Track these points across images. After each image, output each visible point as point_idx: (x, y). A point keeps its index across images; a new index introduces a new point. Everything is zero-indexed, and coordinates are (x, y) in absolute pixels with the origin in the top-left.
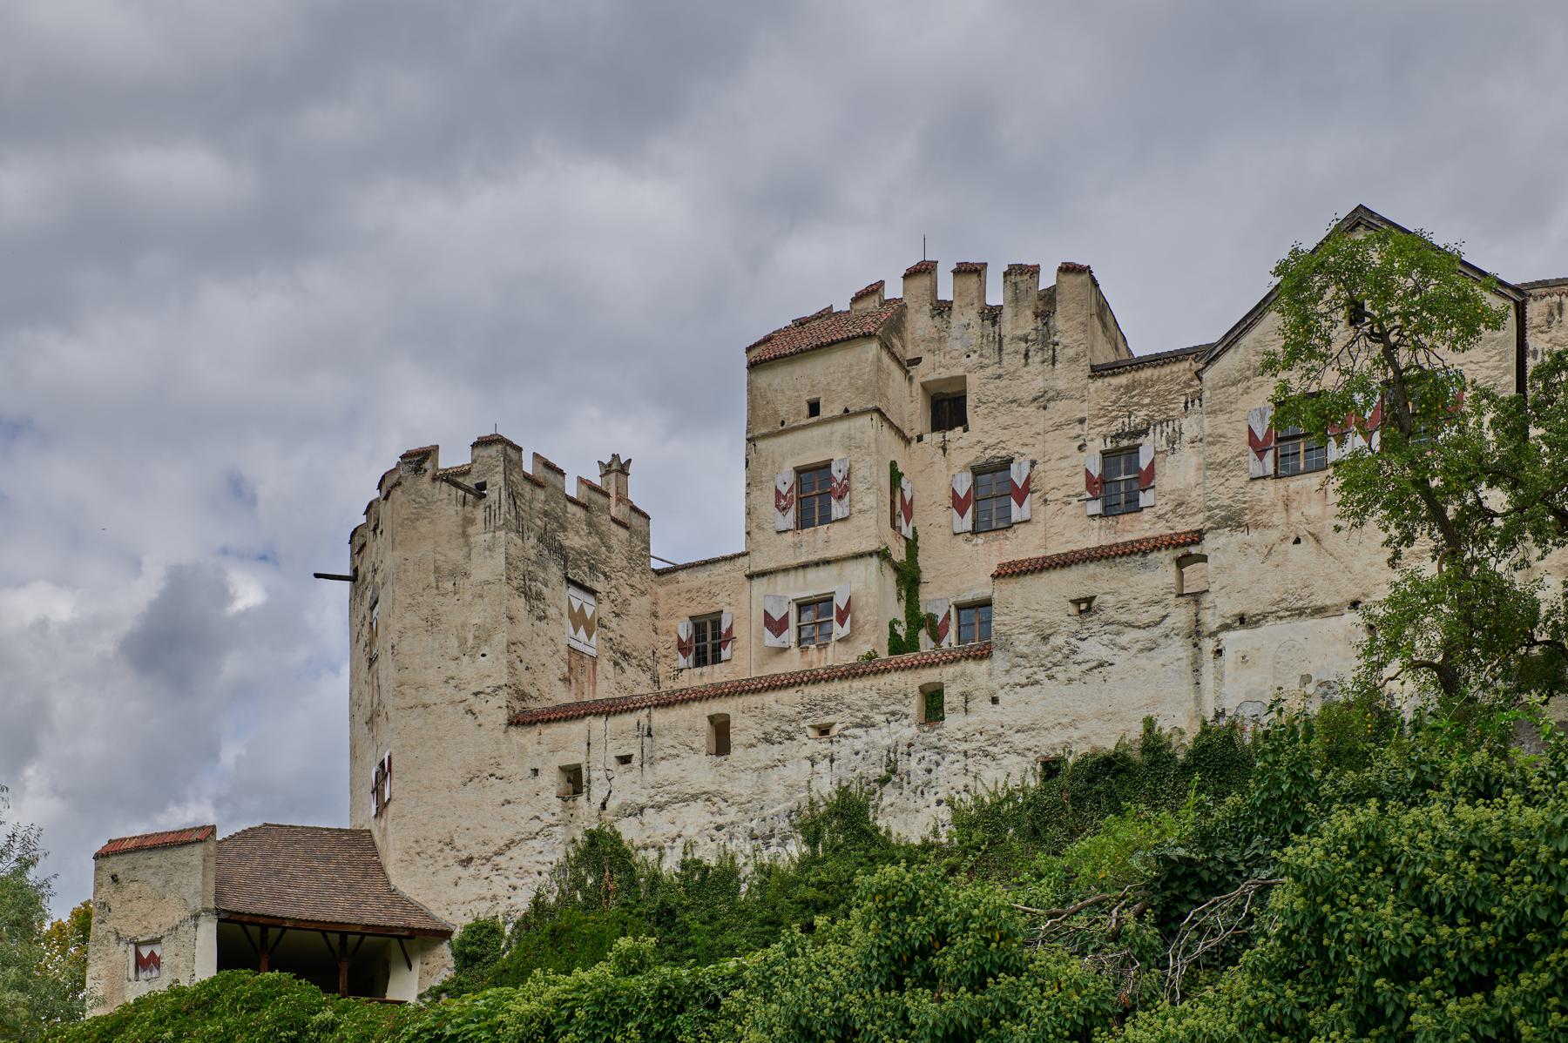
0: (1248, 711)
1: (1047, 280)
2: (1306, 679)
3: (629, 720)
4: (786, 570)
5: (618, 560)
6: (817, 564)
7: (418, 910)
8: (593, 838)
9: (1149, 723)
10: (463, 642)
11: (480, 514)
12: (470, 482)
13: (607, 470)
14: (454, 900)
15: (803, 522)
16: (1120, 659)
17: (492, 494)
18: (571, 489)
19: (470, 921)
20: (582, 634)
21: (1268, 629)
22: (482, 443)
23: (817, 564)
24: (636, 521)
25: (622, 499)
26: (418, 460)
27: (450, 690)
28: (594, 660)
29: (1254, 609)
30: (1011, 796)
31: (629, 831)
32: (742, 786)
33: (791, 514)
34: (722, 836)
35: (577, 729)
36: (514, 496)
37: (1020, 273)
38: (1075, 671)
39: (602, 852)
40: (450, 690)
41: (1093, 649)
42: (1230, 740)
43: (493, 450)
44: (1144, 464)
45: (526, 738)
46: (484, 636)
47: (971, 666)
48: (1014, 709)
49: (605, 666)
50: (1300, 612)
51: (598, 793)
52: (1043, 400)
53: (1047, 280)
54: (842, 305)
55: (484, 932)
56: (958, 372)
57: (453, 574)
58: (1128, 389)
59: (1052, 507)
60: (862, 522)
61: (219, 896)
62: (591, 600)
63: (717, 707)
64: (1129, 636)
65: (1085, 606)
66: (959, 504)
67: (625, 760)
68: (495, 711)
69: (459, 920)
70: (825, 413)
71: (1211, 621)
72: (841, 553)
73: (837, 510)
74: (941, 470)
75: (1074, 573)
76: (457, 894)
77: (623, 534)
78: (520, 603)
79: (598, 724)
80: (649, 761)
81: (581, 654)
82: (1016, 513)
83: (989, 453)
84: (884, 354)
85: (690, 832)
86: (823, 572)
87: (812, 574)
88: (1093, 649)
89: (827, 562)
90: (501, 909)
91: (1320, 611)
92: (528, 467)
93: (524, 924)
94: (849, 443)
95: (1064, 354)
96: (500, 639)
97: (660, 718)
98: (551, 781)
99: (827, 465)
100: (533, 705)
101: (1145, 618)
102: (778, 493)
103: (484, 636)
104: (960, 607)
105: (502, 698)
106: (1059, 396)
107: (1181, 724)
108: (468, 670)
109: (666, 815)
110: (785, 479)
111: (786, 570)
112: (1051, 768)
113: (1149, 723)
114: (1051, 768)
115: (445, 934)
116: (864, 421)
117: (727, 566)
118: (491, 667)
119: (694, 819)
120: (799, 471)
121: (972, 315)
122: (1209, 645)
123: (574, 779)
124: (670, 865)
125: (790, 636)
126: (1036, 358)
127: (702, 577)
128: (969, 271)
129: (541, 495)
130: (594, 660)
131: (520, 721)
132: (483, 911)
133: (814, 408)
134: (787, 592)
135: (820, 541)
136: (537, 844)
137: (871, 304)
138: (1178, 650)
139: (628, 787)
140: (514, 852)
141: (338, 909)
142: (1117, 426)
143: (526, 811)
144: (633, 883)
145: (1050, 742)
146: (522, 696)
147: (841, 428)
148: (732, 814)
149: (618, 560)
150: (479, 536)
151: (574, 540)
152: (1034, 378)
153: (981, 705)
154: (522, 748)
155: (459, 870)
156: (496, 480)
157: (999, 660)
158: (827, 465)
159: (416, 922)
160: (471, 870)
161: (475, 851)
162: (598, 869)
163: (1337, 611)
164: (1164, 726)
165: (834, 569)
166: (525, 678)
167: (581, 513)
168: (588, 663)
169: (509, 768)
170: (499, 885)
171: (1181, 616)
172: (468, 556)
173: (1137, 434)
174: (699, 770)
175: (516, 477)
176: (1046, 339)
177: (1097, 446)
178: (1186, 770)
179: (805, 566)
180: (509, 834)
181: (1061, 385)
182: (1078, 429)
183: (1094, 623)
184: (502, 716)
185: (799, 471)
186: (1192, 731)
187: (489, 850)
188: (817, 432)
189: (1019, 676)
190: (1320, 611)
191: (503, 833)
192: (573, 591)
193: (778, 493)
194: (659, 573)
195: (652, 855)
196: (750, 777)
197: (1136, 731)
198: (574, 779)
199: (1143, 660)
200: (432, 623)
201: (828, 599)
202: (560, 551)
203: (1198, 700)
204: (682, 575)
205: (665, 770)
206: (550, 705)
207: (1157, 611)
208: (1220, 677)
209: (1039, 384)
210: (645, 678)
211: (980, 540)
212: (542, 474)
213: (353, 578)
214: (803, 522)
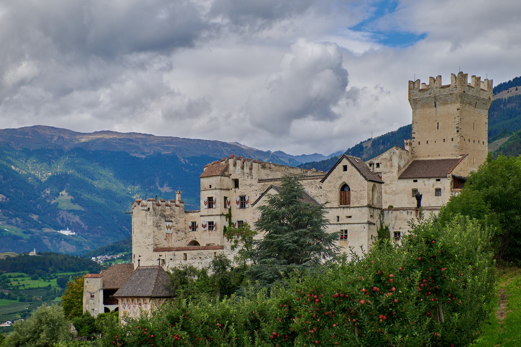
20: (169, 229)
28: (172, 234)
49: (174, 234)
52: (251, 185)
60: (219, 208)
62: (171, 223)
70: (212, 188)
73: (214, 206)
74: (234, 196)
81: (169, 234)
87: (210, 217)
94: (216, 194)
104: (238, 222)
116: (218, 190)
126: (249, 177)
130: (172, 234)
147: (214, 191)
152: (249, 181)
168: (170, 235)
176: (251, 174)
179: (209, 216)
181: (253, 183)
188: (211, 191)
192: (167, 223)
201: (213, 222)
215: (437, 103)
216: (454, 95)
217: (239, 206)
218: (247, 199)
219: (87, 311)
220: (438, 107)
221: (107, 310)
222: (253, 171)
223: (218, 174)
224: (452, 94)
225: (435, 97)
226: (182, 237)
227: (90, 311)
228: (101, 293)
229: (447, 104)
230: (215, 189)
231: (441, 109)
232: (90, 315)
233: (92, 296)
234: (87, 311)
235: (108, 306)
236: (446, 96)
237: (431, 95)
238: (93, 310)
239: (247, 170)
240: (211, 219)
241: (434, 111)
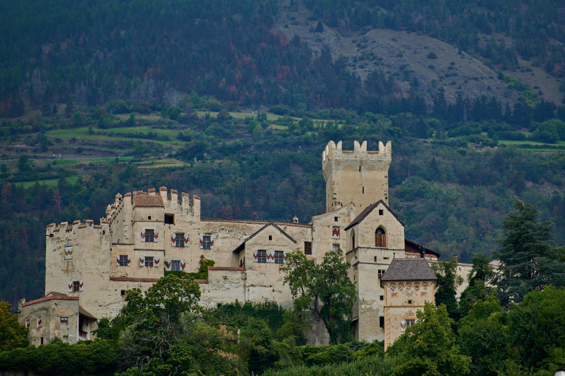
0: (253, 301)
2: (263, 297)
3: (136, 283)
4: (143, 250)
6: (150, 250)
9: (237, 300)
10: (100, 262)
15: (147, 241)
16: (232, 288)
19: (101, 318)
21: (257, 288)
23: (150, 250)
27: (97, 271)
29: (254, 284)
30: (212, 309)
33: (145, 239)
38: (224, 289)
40: (97, 271)
41: (227, 286)
42: (251, 306)
44: (211, 240)
45: (114, 283)
46: (104, 261)
47: (205, 285)
48: (212, 294)
50: (262, 286)
52: (191, 223)
56: (173, 213)
57: (97, 247)
58: (208, 224)
59: (193, 245)
64: (233, 285)
65: (225, 278)
66: (173, 240)
70: (152, 219)
71: (247, 285)
72: (156, 249)
73: (155, 240)
75: (224, 272)
82: (185, 245)
83: (179, 231)
86: (151, 252)
87: (149, 252)
88: (227, 286)
89: (153, 250)
90: (108, 316)
91: (265, 286)
94: (158, 227)
95: (195, 215)
99: (153, 230)
101: (236, 282)
102: (142, 234)
103: (104, 261)
106: (194, 223)
107: (242, 301)
108: (100, 267)
111: (143, 250)
112: (219, 305)
113: (237, 300)
114: (219, 305)
115: (96, 320)
117: (129, 246)
120: (147, 230)
122: (247, 289)
125: (144, 264)
126: (189, 214)
127: (123, 247)
131: (112, 279)
132: (104, 316)
133: (150, 218)
134: (143, 255)
135: (150, 245)
138: (242, 288)
140: (111, 305)
142: (206, 232)
143: (114, 298)
145: (219, 301)
152: (189, 218)
153: (206, 292)
154: (113, 285)
155: (99, 307)
157: (210, 285)
158: (153, 230)
160: (102, 308)
161: (102, 304)
163: (268, 287)
164: (239, 301)
165: (154, 252)
169: (110, 288)
170: (108, 312)
171: (242, 283)
172: (101, 244)
173: (210, 234)
176: (191, 211)
177: (202, 235)
178: (243, 309)
179: (148, 250)
180: (110, 302)
181: (195, 221)
182: (198, 230)
183: (227, 281)
184: (109, 278)
185: (146, 230)
186: (244, 303)
187: (105, 304)
189: (214, 288)
190: (265, 286)
191: (108, 301)
193: (142, 234)
197: (234, 301)
199: (236, 289)
200: (93, 257)
203: (245, 298)
204: (118, 246)
207: (238, 281)
208: (249, 294)
209: (190, 219)
211: (177, 248)
214: (147, 241)
216: (383, 163)
217: (175, 244)
218: (186, 237)
220: (363, 171)
222: (194, 208)
224: (381, 161)
229: (373, 169)
230: (157, 221)
231: (365, 173)
236: (375, 162)
239: (185, 205)
240: (150, 254)
241: (359, 175)
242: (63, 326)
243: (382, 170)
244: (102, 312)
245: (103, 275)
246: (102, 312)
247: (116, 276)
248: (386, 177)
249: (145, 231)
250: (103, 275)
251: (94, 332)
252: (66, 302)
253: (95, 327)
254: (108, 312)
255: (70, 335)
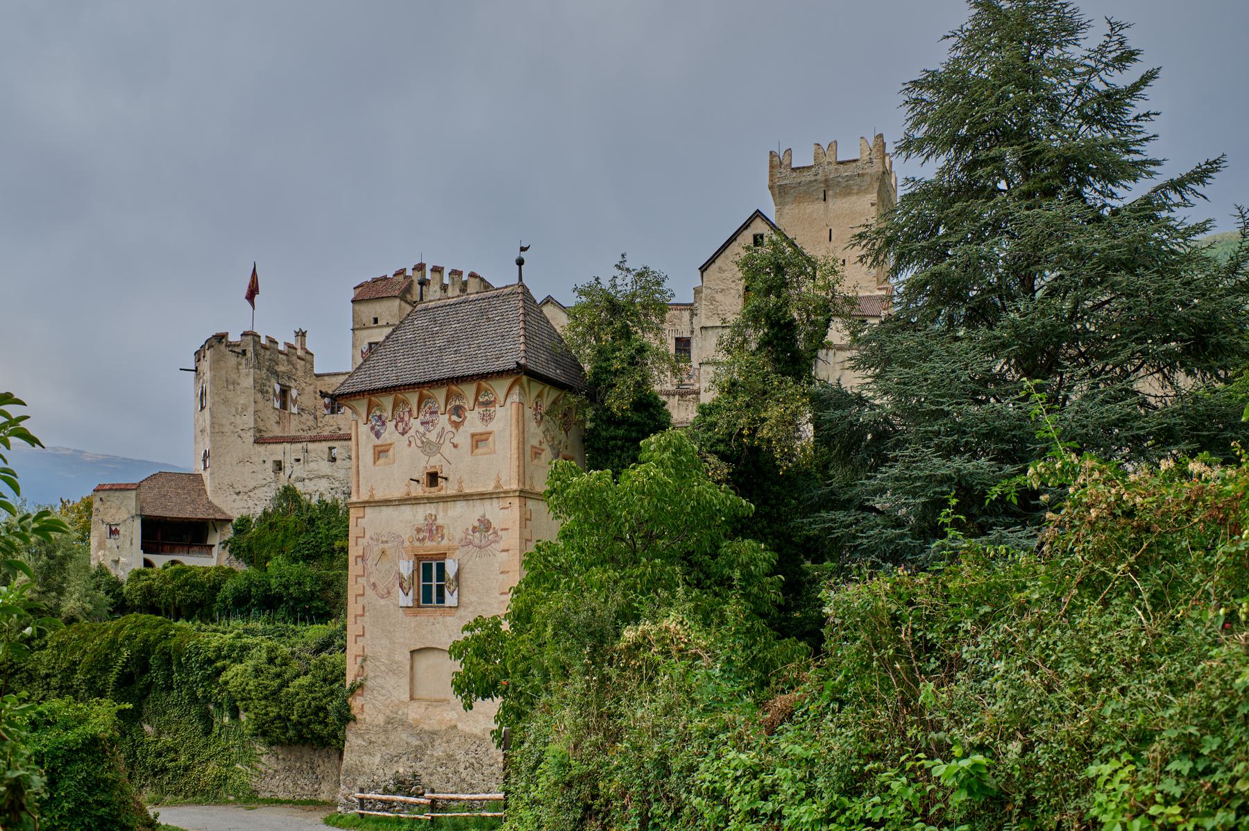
1: (465, 277)
3: (299, 446)
5: (300, 373)
7: (220, 510)
8: (286, 489)
11: (244, 361)
12: (238, 350)
13: (297, 334)
14: (234, 508)
17: (249, 355)
18: (281, 347)
22: (245, 334)
24: (308, 357)
25: (303, 348)
26: (220, 338)
31: (299, 487)
32: (341, 474)
34: (333, 492)
35: (280, 447)
36: (257, 355)
37: (455, 273)
39: (289, 494)
43: (249, 338)
45: (261, 449)
46: (245, 408)
51: (288, 472)
53: (465, 277)
54: (390, 275)
55: (244, 523)
61: (142, 509)
63: (331, 444)
67: (298, 460)
68: (249, 437)
69: (236, 516)
70: (380, 323)
76: (235, 505)
77: (302, 363)
78: (260, 395)
79: (288, 446)
80: (306, 462)
84: (403, 304)
85: (322, 489)
92: (263, 341)
93: (260, 519)
96: (251, 409)
97: (311, 446)
98: (270, 466)
100: (266, 435)
105: (252, 432)
108: (238, 420)
109: (313, 482)
110: (365, 347)
115: (231, 521)
118: (248, 420)
119: (323, 485)
120: (370, 344)
121: (437, 288)
123: (279, 466)
124: (314, 501)
128: (437, 270)
129: (268, 353)
131: (259, 441)
132: (245, 512)
133: (376, 321)
136: (265, 489)
137: (401, 278)
139: (299, 470)
141: (188, 512)
143: (260, 476)
144: (300, 507)
146: (260, 431)
148: (337, 484)
149: (300, 373)
150: (243, 370)
151: (281, 368)
156: (250, 350)
159: (218, 516)
161: (242, 489)
162: (286, 500)
166: (261, 425)
167: (284, 357)
169: (254, 459)
170: (251, 503)
174: (325, 467)
175: (258, 347)
180: (254, 484)
184: (252, 440)
185: (370, 344)
191: (251, 485)
194: (317, 376)
195: (308, 497)
196: (343, 471)
198: (279, 466)
202: (276, 374)
205: (313, 465)
206: (271, 435)
210: (311, 418)
212: (268, 344)
213: (196, 370)
215: (830, 193)
216: (868, 179)
219: (100, 565)
220: (829, 200)
221: (148, 563)
223: (396, 293)
224: (863, 175)
225: (826, 180)
226: (309, 424)
227: (108, 563)
228: (138, 524)
229: (849, 194)
232: (108, 574)
233: (113, 532)
234: (100, 565)
235: (150, 557)
236: (850, 178)
237: (818, 177)
238: (117, 562)
242: (111, 543)
243: (866, 191)
244: (243, 504)
245: (243, 434)
246: (243, 504)
247: (326, 433)
248: (873, 205)
249: (367, 347)
250: (243, 434)
251: (226, 543)
252: (117, 494)
253: (229, 533)
254: (251, 503)
255: (122, 559)
